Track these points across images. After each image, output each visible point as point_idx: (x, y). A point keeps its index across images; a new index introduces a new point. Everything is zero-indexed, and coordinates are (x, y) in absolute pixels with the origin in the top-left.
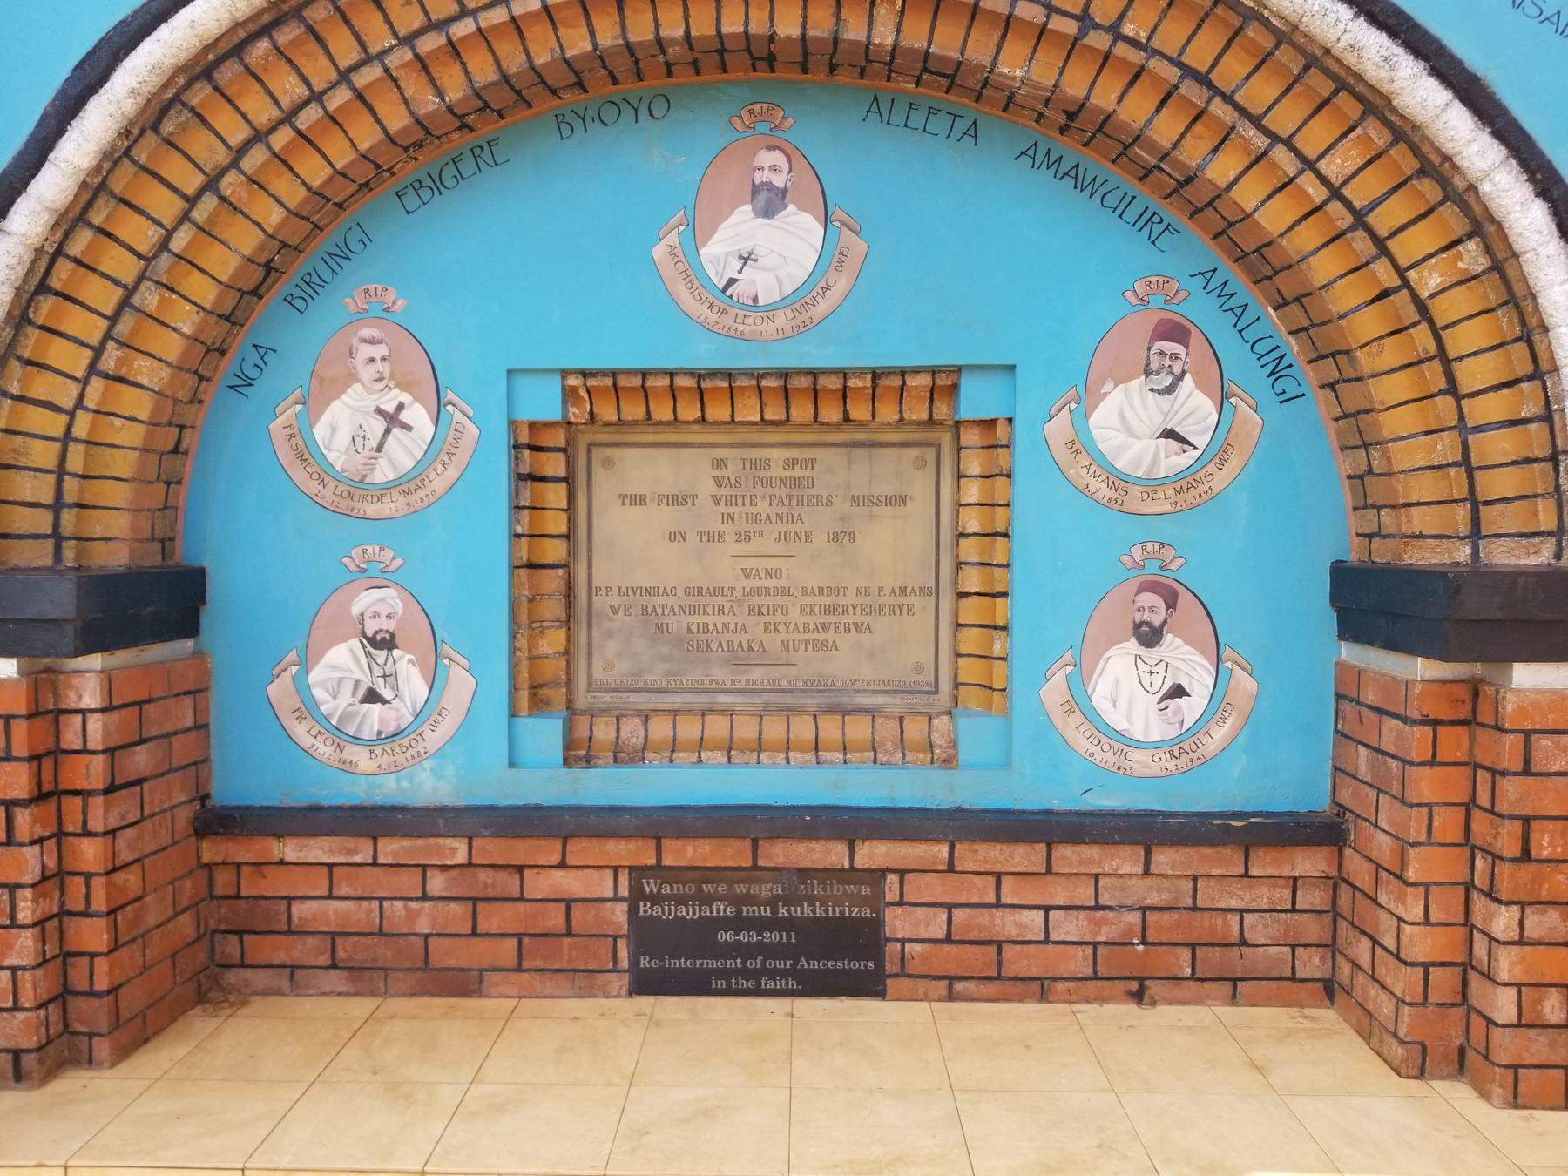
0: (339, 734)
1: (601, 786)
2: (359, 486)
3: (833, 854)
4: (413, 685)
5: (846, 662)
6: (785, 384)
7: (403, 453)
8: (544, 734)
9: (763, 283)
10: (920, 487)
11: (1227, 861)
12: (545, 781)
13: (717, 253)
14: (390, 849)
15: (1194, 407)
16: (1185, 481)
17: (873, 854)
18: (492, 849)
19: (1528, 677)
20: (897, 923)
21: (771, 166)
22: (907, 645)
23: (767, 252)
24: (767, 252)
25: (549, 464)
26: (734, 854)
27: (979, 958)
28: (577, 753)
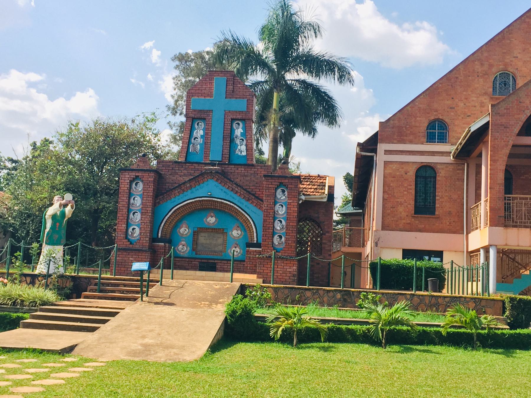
0: (180, 252)
1: (198, 256)
2: (183, 234)
3: (213, 261)
4: (185, 248)
5: (216, 249)
6: (212, 229)
7: (186, 232)
8: (194, 253)
9: (211, 222)
10: (222, 237)
11: (239, 263)
12: (194, 255)
13: (208, 220)
14: (183, 259)
15: (239, 232)
16: (238, 237)
17: (216, 261)
18: (190, 260)
19: (251, 249)
20: (217, 266)
21: (212, 214)
22: (221, 248)
23: (212, 220)
24: (212, 220)
25: (196, 234)
26: (207, 261)
27: (222, 269)
28: (196, 254)
